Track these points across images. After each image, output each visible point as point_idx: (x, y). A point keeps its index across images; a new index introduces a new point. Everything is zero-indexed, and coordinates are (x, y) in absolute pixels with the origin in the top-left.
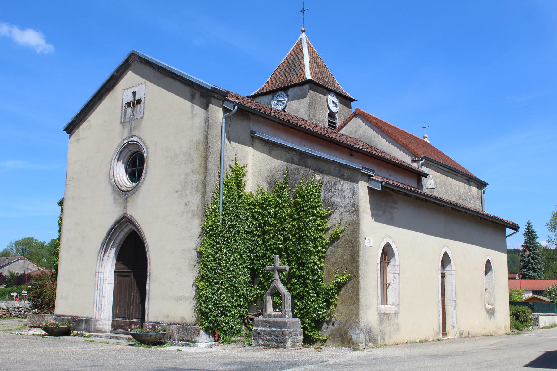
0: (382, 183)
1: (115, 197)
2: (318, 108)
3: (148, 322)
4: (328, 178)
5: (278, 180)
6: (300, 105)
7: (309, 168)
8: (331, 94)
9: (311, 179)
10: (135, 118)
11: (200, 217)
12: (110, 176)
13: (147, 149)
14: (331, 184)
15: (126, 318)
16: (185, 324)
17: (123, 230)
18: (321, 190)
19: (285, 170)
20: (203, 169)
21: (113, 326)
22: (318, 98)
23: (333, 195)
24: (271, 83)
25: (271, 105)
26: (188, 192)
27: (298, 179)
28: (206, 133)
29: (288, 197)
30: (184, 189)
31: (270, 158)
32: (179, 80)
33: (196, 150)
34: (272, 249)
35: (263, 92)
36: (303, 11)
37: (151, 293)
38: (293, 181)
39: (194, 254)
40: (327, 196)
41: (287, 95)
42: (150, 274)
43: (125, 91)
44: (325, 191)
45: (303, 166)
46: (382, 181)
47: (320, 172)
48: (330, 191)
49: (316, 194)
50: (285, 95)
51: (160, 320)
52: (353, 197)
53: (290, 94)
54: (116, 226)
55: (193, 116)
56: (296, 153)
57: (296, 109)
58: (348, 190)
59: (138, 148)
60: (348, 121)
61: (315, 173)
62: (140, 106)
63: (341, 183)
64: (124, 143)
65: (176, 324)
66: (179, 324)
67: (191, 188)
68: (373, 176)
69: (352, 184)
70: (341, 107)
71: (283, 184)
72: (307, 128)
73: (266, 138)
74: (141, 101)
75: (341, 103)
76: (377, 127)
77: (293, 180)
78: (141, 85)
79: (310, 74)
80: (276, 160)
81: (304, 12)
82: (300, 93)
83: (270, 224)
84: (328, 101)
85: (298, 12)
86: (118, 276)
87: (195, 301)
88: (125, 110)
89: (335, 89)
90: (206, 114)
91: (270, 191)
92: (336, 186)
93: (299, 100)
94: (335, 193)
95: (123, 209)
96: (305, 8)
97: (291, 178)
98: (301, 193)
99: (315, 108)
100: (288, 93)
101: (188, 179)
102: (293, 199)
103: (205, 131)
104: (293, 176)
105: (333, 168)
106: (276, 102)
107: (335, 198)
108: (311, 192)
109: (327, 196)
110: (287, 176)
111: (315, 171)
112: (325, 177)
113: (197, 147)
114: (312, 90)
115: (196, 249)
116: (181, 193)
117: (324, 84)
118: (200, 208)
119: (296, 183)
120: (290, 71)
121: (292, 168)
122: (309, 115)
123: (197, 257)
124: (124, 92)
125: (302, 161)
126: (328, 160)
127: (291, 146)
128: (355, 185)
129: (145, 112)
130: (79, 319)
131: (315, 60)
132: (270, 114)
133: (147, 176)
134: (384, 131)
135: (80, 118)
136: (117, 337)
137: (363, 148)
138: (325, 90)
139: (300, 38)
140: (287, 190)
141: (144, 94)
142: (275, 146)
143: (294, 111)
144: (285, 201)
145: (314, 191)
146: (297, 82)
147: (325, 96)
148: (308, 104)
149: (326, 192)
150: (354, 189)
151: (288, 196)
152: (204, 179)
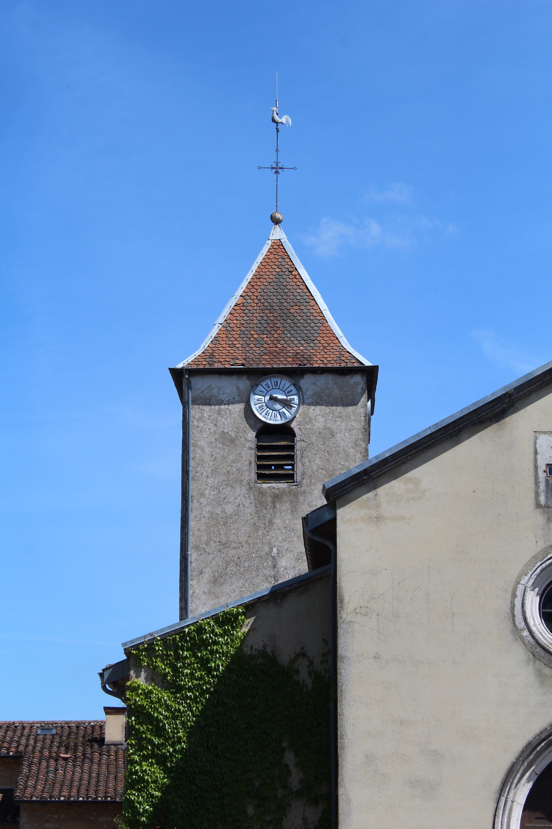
1: (539, 671)
6: (338, 423)
36: (277, 169)
41: (299, 391)
50: (292, 388)
53: (307, 390)
82: (336, 392)
85: (260, 168)
93: (334, 408)
100: (300, 383)
124: (536, 438)
135: (384, 468)
143: (320, 433)
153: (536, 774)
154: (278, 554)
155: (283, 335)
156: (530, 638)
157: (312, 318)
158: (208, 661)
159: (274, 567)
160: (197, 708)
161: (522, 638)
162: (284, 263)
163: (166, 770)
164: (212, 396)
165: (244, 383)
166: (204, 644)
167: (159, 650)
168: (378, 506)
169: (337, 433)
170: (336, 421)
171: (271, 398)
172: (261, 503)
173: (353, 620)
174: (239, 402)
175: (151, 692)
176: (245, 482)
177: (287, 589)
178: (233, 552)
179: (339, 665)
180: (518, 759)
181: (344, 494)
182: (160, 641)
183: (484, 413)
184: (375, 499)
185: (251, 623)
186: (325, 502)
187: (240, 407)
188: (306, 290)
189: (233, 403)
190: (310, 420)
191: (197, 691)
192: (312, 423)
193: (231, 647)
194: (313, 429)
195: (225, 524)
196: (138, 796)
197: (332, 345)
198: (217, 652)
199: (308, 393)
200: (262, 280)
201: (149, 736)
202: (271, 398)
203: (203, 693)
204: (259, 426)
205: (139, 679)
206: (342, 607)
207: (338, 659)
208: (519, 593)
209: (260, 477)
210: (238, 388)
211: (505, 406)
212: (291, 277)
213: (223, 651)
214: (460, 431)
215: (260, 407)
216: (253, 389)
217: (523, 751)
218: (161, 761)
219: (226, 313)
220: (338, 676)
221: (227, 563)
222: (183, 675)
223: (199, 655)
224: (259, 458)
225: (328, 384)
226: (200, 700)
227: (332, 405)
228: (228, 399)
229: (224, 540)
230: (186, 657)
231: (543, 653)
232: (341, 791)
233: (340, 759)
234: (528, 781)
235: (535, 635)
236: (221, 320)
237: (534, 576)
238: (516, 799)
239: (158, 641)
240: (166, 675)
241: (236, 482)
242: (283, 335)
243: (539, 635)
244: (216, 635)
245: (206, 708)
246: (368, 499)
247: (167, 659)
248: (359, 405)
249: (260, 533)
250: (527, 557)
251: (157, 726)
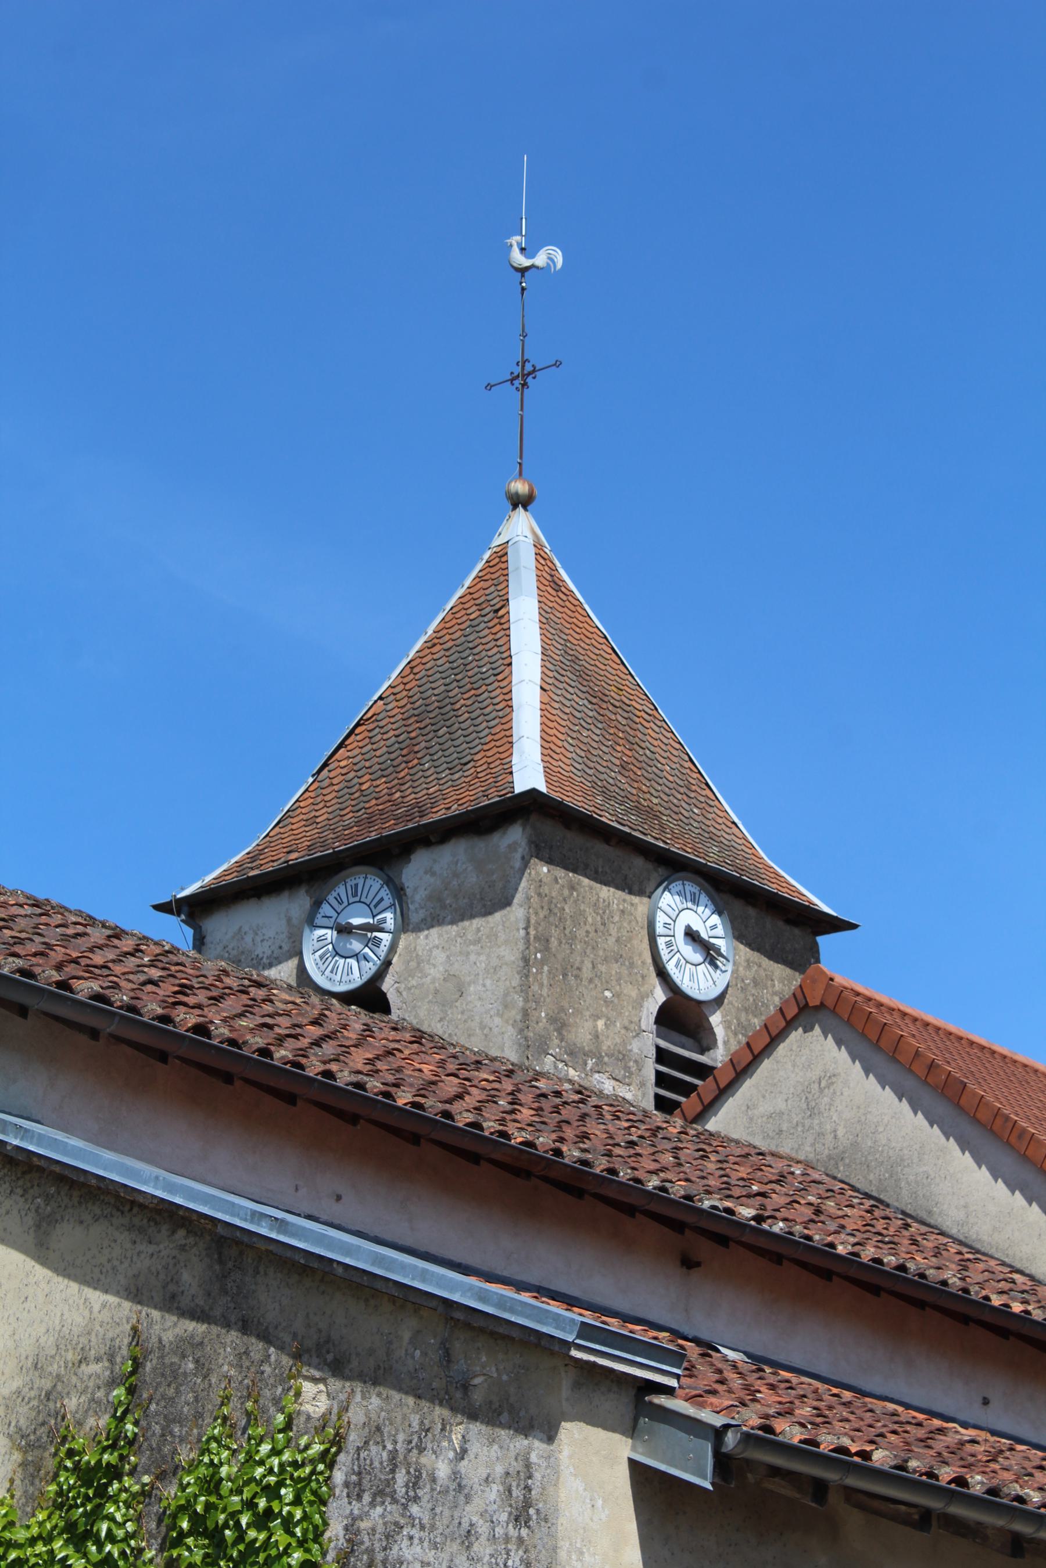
0: (718, 1434)
2: (587, 972)
4: (375, 1401)
5: (80, 1424)
7: (266, 1337)
8: (677, 886)
9: (272, 1410)
14: (390, 1447)
18: (331, 1489)
19: (125, 1352)
22: (589, 910)
23: (402, 1521)
24: (312, 821)
25: (300, 954)
27: (199, 1416)
29: (129, 1536)
31: (41, 1272)
35: (256, 872)
38: (166, 1431)
40: (364, 1525)
41: (399, 892)
44: (354, 1491)
45: (228, 1325)
46: (718, 1421)
47: (329, 1365)
48: (383, 1493)
49: (298, 1514)
50: (385, 894)
52: (524, 1532)
53: (416, 889)
56: (191, 1240)
57: (449, 977)
58: (495, 1487)
60: (756, 1051)
61: (299, 1375)
63: (450, 1441)
68: (669, 1391)
69: (521, 1443)
70: (748, 967)
71: (104, 1450)
72: (340, 1083)
73: (16, 1142)
75: (749, 945)
76: (934, 1088)
77: (169, 1420)
79: (538, 757)
80: (74, 1286)
81: (524, 385)
82: (472, 879)
84: (660, 929)
85: (489, 387)
89: (712, 858)
91: (28, 1497)
92: (423, 1460)
93: (466, 923)
94: (414, 1509)
96: (536, 359)
97: (153, 1407)
98: (209, 1507)
99: (568, 970)
100: (404, 880)
102: (161, 1549)
104: (171, 1392)
105: (407, 1336)
106: (330, 934)
107: (411, 1538)
108: (262, 1503)
109: (364, 1525)
110: (131, 1391)
111: (297, 1356)
112: (358, 1397)
114: (550, 861)
117: (630, 824)
119: (182, 1440)
120: (423, 744)
121: (164, 1338)
122: (526, 1014)
125: (224, 1291)
126: (379, 1285)
127: (159, 1193)
128: (537, 1448)
131: (582, 675)
132: (63, 985)
134: (979, 1115)
137: (759, 1219)
138: (639, 862)
139: (497, 541)
140: (126, 1490)
142: (76, 1193)
145: (283, 1491)
146: (455, 809)
147: (636, 899)
148: (521, 946)
149: (359, 1497)
150: (530, 1477)
151: (130, 1527)
164: (243, 953)
169: (469, 984)
170: (468, 954)
190: (419, 964)
192: (421, 971)
194: (423, 984)
199: (418, 898)
225: (457, 863)
228: (270, 952)
248: (515, 901)
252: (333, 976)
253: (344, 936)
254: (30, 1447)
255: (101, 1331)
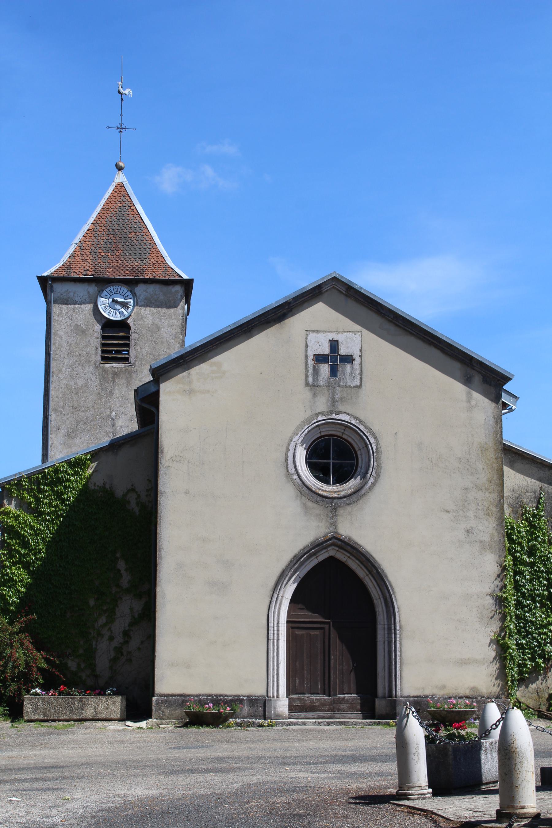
1: (304, 504)
3: (401, 697)
6: (163, 320)
10: (342, 383)
11: (495, 551)
12: (287, 468)
13: (375, 438)
15: (318, 694)
16: (479, 696)
17: (317, 557)
20: (496, 486)
21: (291, 708)
26: (471, 514)
28: (498, 437)
30: (462, 510)
32: (436, 347)
33: (480, 457)
34: (530, 595)
36: (121, 129)
37: (403, 655)
39: (490, 601)
42: (400, 627)
43: (311, 336)
50: (129, 293)
51: (427, 692)
53: (140, 295)
54: (313, 550)
55: (470, 408)
59: (343, 431)
62: (352, 368)
64: (319, 419)
65: (462, 697)
66: (467, 697)
67: (476, 509)
74: (354, 360)
78: (350, 335)
80: (522, 476)
82: (162, 297)
83: (524, 563)
85: (108, 127)
86: (292, 628)
87: (496, 664)
88: (314, 367)
90: (496, 410)
93: (160, 309)
95: (328, 524)
101: (469, 496)
103: (496, 433)
113: (482, 453)
115: (491, 595)
116: (458, 514)
118: (495, 539)
121: (549, 491)
123: (496, 605)
124: (307, 335)
129: (363, 380)
130: (231, 700)
133: (381, 481)
135: (195, 354)
136: (344, 722)
141: (361, 350)
143: (149, 327)
144: (544, 534)
152: (500, 500)
153: (300, 578)
154: (116, 416)
155: (123, 254)
156: (298, 480)
157: (145, 241)
158: (62, 493)
159: (113, 426)
160: (53, 528)
161: (292, 480)
162: (125, 200)
163: (30, 573)
164: (69, 298)
165: (93, 289)
166: (60, 481)
167: (26, 485)
168: (190, 382)
169: (162, 328)
170: (161, 319)
171: (113, 301)
172: (104, 378)
173: (170, 465)
174: (89, 303)
175: (19, 516)
176: (92, 363)
177: (122, 441)
178: (83, 414)
179: (160, 498)
180: (287, 567)
181: (165, 373)
182: (26, 478)
183: (270, 316)
184: (188, 377)
185: (95, 466)
186: (152, 379)
187: (90, 306)
188: (141, 221)
189: (85, 303)
191: (54, 515)
193: (80, 483)
194: (144, 324)
195: (77, 393)
196: (8, 591)
197: (159, 262)
198: (69, 487)
199: (141, 298)
200: (108, 212)
201: (17, 548)
202: (113, 301)
203: (58, 517)
204: (104, 321)
205: (11, 506)
206: (162, 456)
207: (159, 493)
208: (292, 448)
209: (104, 359)
210: (88, 293)
211: (285, 311)
212: (130, 210)
213: (73, 487)
214: (252, 328)
215: (104, 307)
216: (99, 293)
217: (291, 561)
218: (26, 566)
219: (80, 236)
220: (158, 506)
221: (78, 422)
222: (43, 504)
223: (56, 489)
224: (103, 345)
225: (156, 291)
226: (56, 522)
227: (158, 307)
228: (81, 300)
229: (76, 405)
230: (46, 491)
231: (307, 491)
232: (158, 589)
233: (158, 566)
234: (294, 583)
235: (302, 478)
236: (77, 241)
237: (303, 436)
238: (285, 595)
239: (25, 478)
240: (31, 503)
241: (85, 362)
242: (123, 254)
243: (305, 478)
244: (68, 475)
245: (60, 527)
246: (183, 377)
247: (31, 492)
249: (103, 400)
250: (298, 423)
251: (23, 541)
252: (109, 314)
253: (114, 303)
254: (513, 508)
255: (531, 487)
